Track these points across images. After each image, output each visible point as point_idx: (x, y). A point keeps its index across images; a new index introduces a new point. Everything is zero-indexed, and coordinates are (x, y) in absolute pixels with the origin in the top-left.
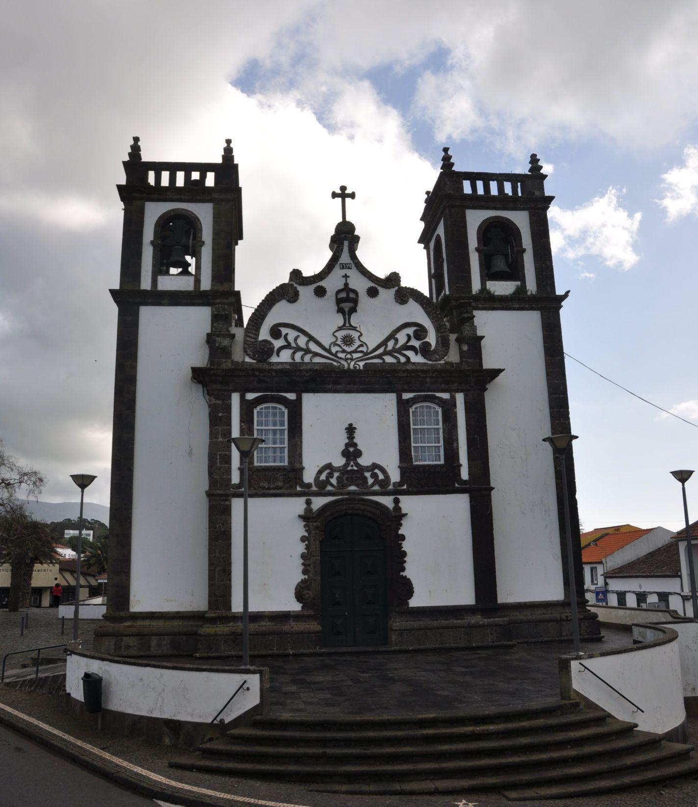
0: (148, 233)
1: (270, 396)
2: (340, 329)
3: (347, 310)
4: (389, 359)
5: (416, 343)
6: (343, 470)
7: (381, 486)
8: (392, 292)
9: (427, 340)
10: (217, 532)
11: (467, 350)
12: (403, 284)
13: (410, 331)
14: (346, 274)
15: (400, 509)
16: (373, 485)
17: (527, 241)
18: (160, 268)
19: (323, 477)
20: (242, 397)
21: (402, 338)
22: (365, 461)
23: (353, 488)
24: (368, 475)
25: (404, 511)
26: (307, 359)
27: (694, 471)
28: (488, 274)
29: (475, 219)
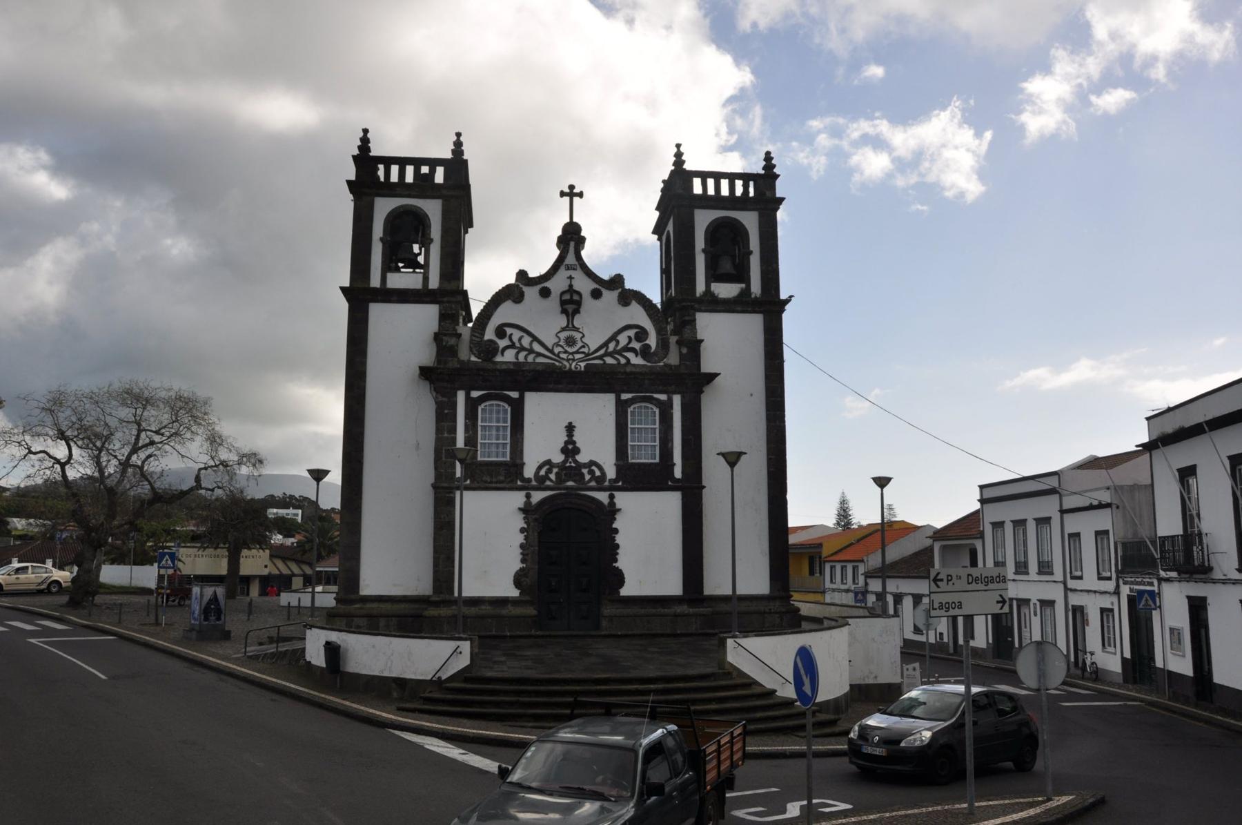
2: (563, 330)
3: (570, 311)
4: (609, 360)
6: (562, 466)
7: (597, 482)
8: (616, 293)
9: (647, 342)
12: (628, 285)
13: (631, 333)
14: (571, 276)
15: (615, 504)
16: (590, 480)
17: (754, 243)
18: (389, 266)
19: (542, 472)
20: (468, 397)
21: (623, 340)
22: (582, 458)
23: (570, 483)
24: (585, 471)
25: (618, 506)
26: (530, 359)
28: (714, 275)
29: (703, 219)
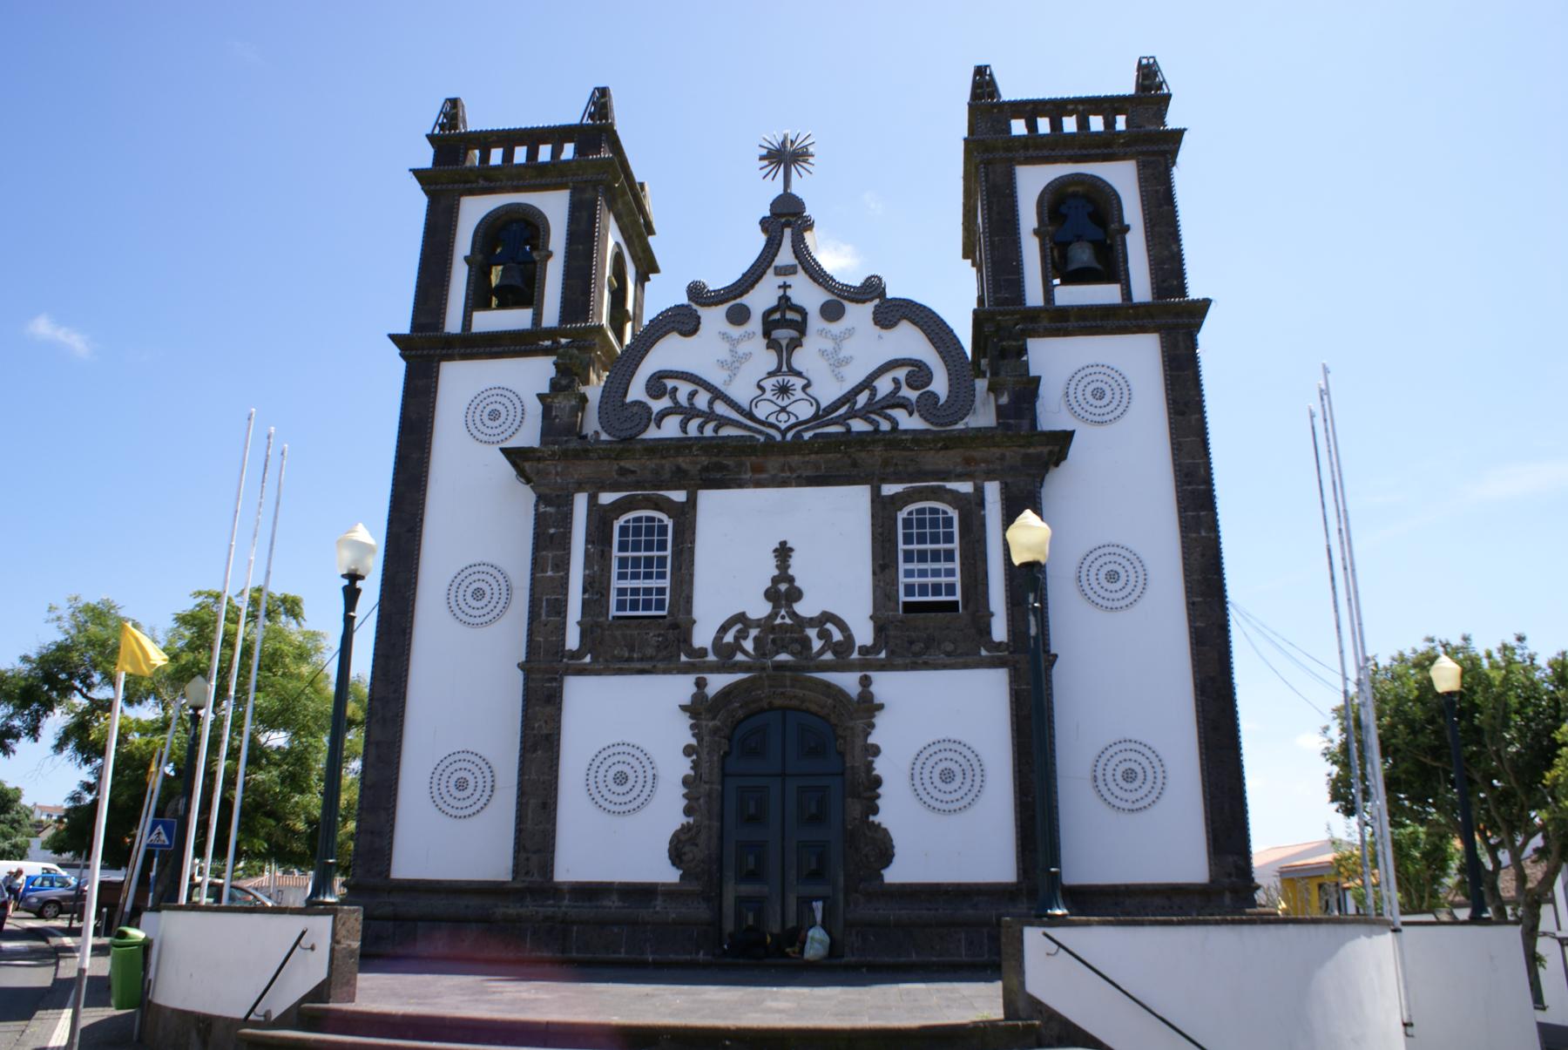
0: (463, 244)
1: (640, 497)
2: (771, 374)
3: (784, 343)
4: (858, 425)
5: (913, 395)
6: (766, 625)
7: (835, 653)
8: (869, 307)
9: (930, 388)
10: (535, 736)
11: (1009, 403)
12: (891, 293)
13: (901, 373)
14: (785, 283)
15: (871, 695)
16: (822, 651)
17: (1132, 212)
18: (479, 298)
19: (729, 638)
20: (592, 500)
21: (884, 386)
22: (806, 608)
23: (783, 657)
24: (812, 633)
25: (878, 700)
26: (709, 431)
27: (1185, 129)
28: (1060, 268)
29: (1032, 182)
